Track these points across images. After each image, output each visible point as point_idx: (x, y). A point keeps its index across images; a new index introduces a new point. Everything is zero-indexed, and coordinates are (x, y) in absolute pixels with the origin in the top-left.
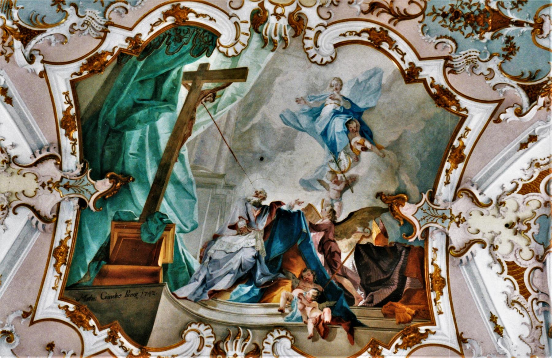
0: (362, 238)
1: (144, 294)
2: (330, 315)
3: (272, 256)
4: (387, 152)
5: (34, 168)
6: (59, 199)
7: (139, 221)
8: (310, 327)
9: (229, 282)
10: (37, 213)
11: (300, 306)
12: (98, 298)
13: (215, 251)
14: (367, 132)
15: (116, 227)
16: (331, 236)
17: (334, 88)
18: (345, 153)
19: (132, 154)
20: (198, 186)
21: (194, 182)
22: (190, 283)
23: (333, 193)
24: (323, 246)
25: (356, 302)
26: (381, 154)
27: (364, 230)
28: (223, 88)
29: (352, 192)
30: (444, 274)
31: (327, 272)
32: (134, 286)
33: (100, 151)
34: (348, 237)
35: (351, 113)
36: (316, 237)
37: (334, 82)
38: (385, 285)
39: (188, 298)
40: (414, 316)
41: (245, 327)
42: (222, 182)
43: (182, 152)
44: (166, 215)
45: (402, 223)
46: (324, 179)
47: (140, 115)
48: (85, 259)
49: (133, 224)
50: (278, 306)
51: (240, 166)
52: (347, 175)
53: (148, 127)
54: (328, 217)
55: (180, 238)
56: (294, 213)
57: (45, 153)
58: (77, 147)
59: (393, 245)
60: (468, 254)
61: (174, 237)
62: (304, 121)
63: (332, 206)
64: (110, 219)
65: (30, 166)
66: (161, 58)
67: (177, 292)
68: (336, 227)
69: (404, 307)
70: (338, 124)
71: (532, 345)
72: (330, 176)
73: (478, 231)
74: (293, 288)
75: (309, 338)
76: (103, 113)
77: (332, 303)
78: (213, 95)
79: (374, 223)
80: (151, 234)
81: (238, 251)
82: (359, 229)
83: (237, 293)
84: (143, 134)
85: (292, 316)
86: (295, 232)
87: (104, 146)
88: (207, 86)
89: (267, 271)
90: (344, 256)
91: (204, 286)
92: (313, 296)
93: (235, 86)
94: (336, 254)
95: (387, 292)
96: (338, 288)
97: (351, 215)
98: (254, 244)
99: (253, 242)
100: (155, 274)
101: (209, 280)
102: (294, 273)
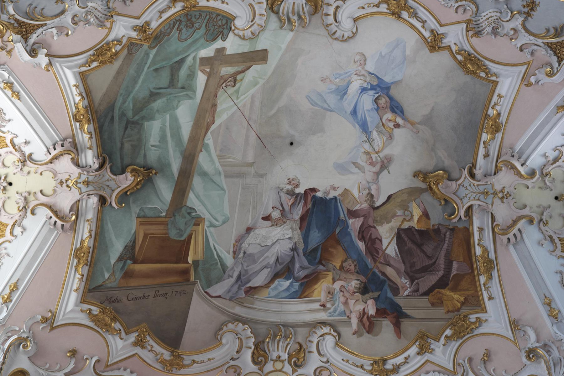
0: (403, 222)
1: (174, 293)
2: (375, 307)
3: (310, 248)
4: (420, 127)
5: (50, 165)
6: (78, 197)
7: (166, 217)
8: (355, 321)
9: (266, 277)
10: (55, 213)
11: (342, 299)
13: (249, 245)
14: (397, 107)
15: (142, 224)
17: (358, 63)
18: (377, 131)
19: (153, 146)
20: (226, 177)
21: (222, 172)
22: (224, 280)
23: (369, 176)
24: (363, 234)
26: (415, 130)
27: (404, 213)
28: (243, 71)
29: (389, 173)
30: (492, 256)
31: (369, 261)
33: (119, 144)
34: (388, 223)
35: (378, 89)
37: (358, 58)
38: (431, 271)
39: (222, 296)
40: (463, 304)
41: (286, 326)
42: (252, 170)
43: (206, 141)
44: (194, 209)
45: (443, 202)
46: (359, 161)
47: (158, 104)
48: (109, 259)
49: (160, 220)
50: (319, 301)
51: (269, 152)
52: (381, 155)
53: (168, 116)
54: (366, 201)
55: (210, 233)
56: (331, 199)
57: (59, 149)
58: (94, 140)
59: (436, 227)
61: (204, 231)
62: (332, 100)
63: (369, 189)
64: (134, 216)
65: (47, 164)
66: (174, 45)
67: (209, 290)
68: (374, 212)
69: (452, 294)
70: (367, 101)
72: (364, 157)
74: (334, 281)
75: (354, 334)
76: (118, 105)
77: (376, 294)
78: (234, 79)
79: (414, 204)
80: (180, 229)
81: (273, 244)
82: (399, 212)
83: (276, 288)
84: (164, 124)
85: (335, 311)
86: (332, 220)
87: (122, 139)
88: (226, 70)
91: (239, 283)
92: (355, 287)
93: (256, 69)
94: (377, 241)
95: (433, 279)
96: (382, 277)
98: (290, 236)
99: (289, 233)
100: (186, 272)
101: (244, 276)
102: (334, 264)
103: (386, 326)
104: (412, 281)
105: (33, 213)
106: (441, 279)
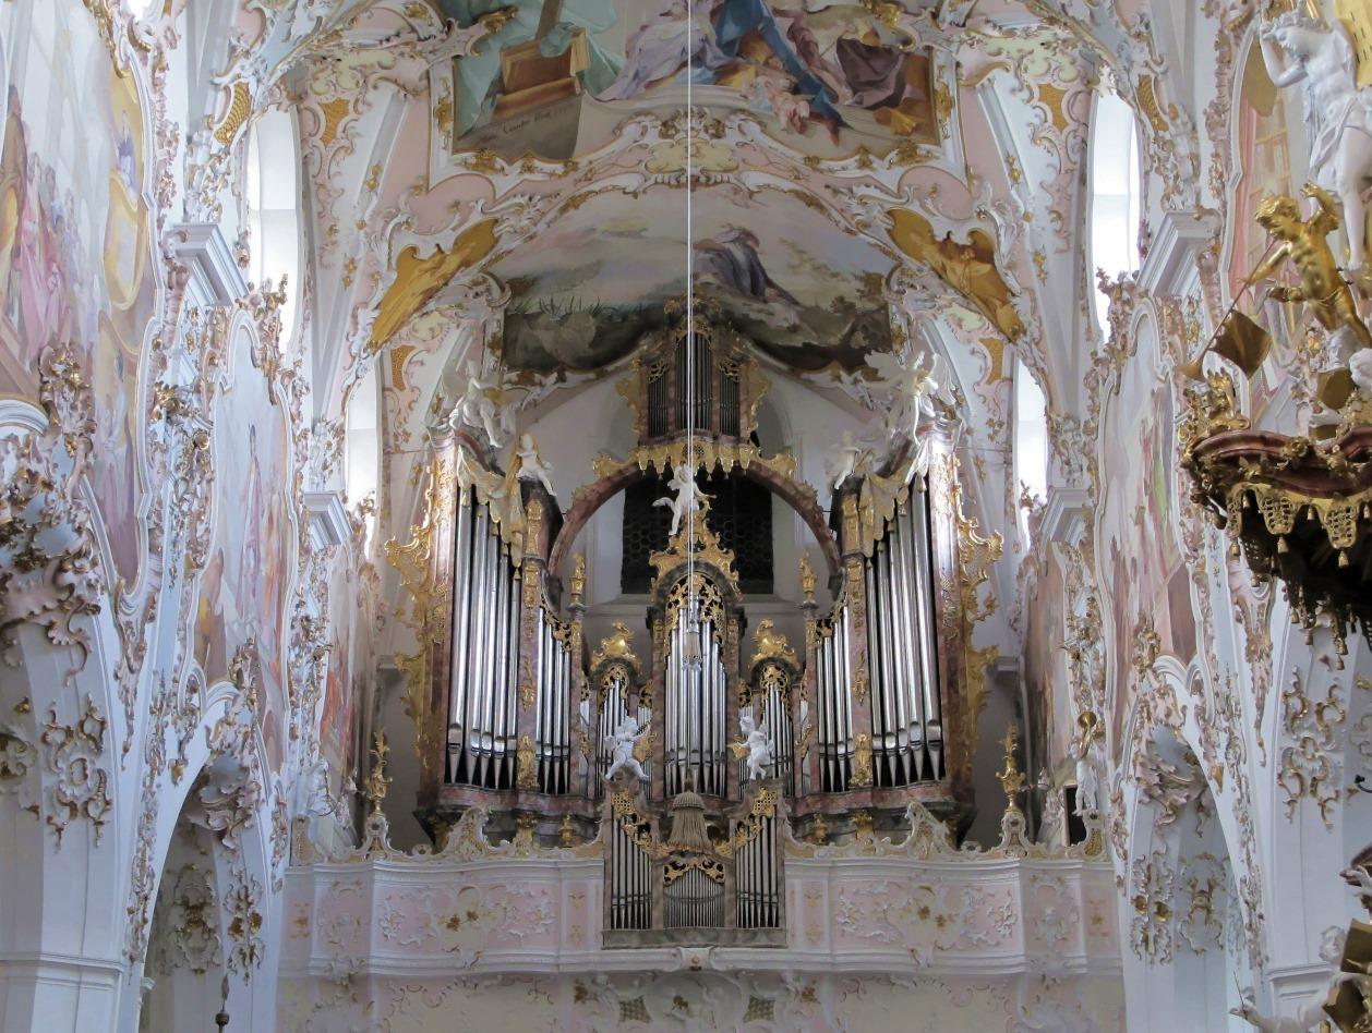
8: (783, 120)
12: (501, 133)
15: (508, 55)
16: (803, 24)
24: (793, 33)
25: (841, 99)
31: (802, 63)
36: (781, 25)
40: (915, 129)
60: (984, 81)
67: (601, 96)
71: (1058, 195)
73: (999, 53)
74: (757, 74)
77: (810, 97)
89: (721, 54)
90: (822, 48)
95: (881, 95)
96: (818, 82)
97: (827, 8)
100: (569, 88)
103: (821, 131)
104: (855, 93)
105: (375, 87)
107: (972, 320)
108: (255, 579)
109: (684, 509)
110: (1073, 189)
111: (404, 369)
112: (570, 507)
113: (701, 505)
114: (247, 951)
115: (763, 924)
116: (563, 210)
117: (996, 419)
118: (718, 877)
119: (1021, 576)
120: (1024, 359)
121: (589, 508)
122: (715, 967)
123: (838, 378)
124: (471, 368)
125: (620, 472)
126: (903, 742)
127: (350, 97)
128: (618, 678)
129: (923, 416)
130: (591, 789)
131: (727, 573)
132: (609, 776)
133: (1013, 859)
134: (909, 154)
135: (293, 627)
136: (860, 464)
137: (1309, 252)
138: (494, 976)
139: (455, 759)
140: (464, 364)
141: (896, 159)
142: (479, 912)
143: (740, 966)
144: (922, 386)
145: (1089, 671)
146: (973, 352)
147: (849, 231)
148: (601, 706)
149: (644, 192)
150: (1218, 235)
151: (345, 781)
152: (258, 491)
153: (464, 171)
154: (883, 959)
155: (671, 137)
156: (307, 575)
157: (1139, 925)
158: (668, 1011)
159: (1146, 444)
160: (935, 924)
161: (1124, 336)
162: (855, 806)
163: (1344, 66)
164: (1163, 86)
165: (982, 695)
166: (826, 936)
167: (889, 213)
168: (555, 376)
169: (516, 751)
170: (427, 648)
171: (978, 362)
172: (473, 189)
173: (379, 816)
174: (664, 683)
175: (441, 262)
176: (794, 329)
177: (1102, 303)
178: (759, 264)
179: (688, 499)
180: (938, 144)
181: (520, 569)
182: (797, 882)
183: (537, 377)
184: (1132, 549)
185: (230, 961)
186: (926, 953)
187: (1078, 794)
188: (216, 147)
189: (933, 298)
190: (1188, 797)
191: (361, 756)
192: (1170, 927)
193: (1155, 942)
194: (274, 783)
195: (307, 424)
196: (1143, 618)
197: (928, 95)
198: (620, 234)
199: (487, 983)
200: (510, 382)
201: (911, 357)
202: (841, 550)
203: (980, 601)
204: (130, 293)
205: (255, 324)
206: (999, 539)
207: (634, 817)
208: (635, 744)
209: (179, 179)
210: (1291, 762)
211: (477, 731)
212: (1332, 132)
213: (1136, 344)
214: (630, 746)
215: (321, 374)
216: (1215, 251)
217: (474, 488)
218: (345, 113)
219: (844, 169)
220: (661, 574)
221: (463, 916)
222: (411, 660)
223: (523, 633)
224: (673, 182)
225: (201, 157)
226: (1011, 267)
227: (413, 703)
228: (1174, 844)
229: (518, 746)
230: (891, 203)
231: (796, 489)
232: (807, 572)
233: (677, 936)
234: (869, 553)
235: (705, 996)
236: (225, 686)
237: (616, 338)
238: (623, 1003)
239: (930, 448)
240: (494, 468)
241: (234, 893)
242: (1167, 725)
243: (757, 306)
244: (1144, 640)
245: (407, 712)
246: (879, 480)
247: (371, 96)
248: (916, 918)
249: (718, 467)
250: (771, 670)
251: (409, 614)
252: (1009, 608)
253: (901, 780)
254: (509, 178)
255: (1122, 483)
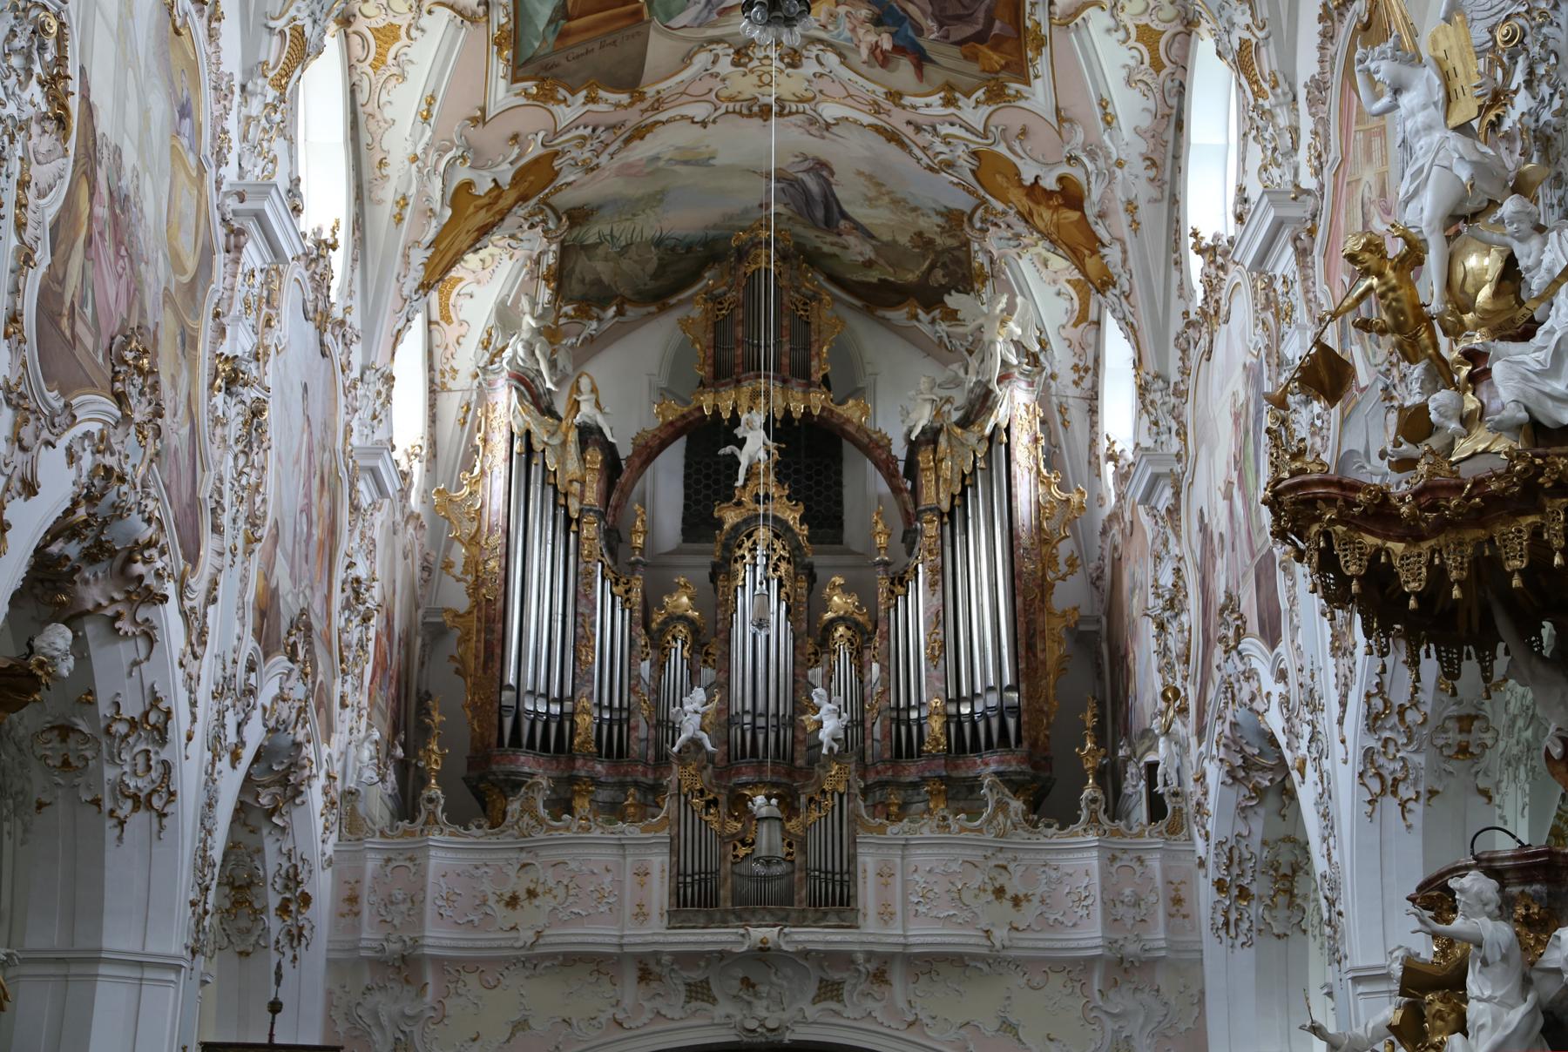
8: (864, 52)
11: (849, 25)
30: (1045, 30)
32: (610, 33)
40: (1003, 68)
67: (672, 24)
77: (894, 29)
85: (839, 35)
95: (969, 31)
100: (638, 12)
104: (941, 26)
105: (430, 12)
106: (979, 33)
107: (1059, 263)
108: (307, 545)
109: (751, 458)
110: (1170, 135)
111: (452, 301)
112: (630, 452)
113: (768, 453)
114: (295, 931)
115: (834, 904)
116: (627, 141)
117: (1081, 364)
118: (789, 854)
119: (1104, 532)
120: (1113, 311)
121: (648, 451)
122: (785, 947)
123: (915, 317)
124: (525, 304)
125: (683, 416)
126: (979, 708)
127: (403, 21)
128: (681, 637)
129: (1004, 363)
130: (651, 752)
131: (797, 528)
132: (675, 749)
133: (1092, 838)
134: (996, 95)
135: (343, 590)
136: (938, 413)
137: (1393, 289)
138: (554, 956)
139: (508, 722)
140: (517, 300)
141: (983, 98)
142: (540, 890)
143: (810, 946)
144: (1004, 332)
145: (1175, 644)
146: (1059, 294)
147: (931, 169)
148: (662, 667)
149: (714, 122)
150: (1314, 216)
151: (391, 745)
152: (310, 452)
153: (524, 101)
154: (957, 940)
155: (745, 65)
156: (357, 533)
157: (1219, 907)
158: (735, 992)
159: (1237, 417)
160: (1010, 904)
161: (1217, 301)
162: (927, 774)
163: (1435, 104)
164: (1263, 51)
165: (1062, 658)
166: (899, 914)
167: (975, 154)
168: (612, 311)
169: (573, 714)
170: (478, 604)
171: (1063, 304)
172: (535, 123)
173: (434, 790)
174: (728, 641)
175: (499, 197)
176: (869, 264)
177: (1196, 264)
178: (833, 195)
179: (755, 446)
180: (1028, 84)
181: (578, 521)
182: (868, 859)
183: (595, 311)
184: (1219, 524)
185: (278, 942)
186: (1001, 935)
187: (1160, 770)
188: (272, 94)
189: (1018, 236)
190: (1271, 780)
191: (408, 715)
192: (1252, 911)
193: (1237, 926)
194: (325, 757)
195: (356, 374)
196: (1229, 597)
197: (1019, 32)
198: (686, 163)
199: (548, 964)
200: (566, 315)
201: (993, 301)
202: (916, 504)
203: (1061, 560)
204: (191, 264)
205: (307, 274)
206: (1082, 493)
207: (702, 792)
208: (704, 715)
209: (234, 135)
210: (1372, 762)
211: (532, 693)
212: (1421, 169)
213: (1229, 312)
214: (697, 718)
215: (370, 318)
216: (1311, 233)
217: (528, 433)
218: (397, 38)
219: (927, 106)
220: (726, 527)
221: (522, 895)
222: (461, 616)
223: (581, 589)
224: (745, 111)
225: (255, 107)
226: (1102, 215)
227: (462, 661)
228: (1257, 826)
229: (575, 708)
230: (977, 143)
231: (869, 437)
232: (880, 527)
233: (746, 916)
234: (945, 506)
235: (774, 979)
236: (280, 661)
237: (676, 270)
238: (689, 985)
239: (1012, 398)
240: (549, 411)
241: (283, 872)
242: (1251, 709)
243: (830, 239)
244: (1230, 619)
245: (457, 672)
246: (959, 431)
247: (425, 21)
248: (991, 897)
249: (788, 412)
250: (841, 630)
251: (458, 570)
252: (1092, 565)
253: (975, 747)
254: (571, 110)
255: (1211, 454)
